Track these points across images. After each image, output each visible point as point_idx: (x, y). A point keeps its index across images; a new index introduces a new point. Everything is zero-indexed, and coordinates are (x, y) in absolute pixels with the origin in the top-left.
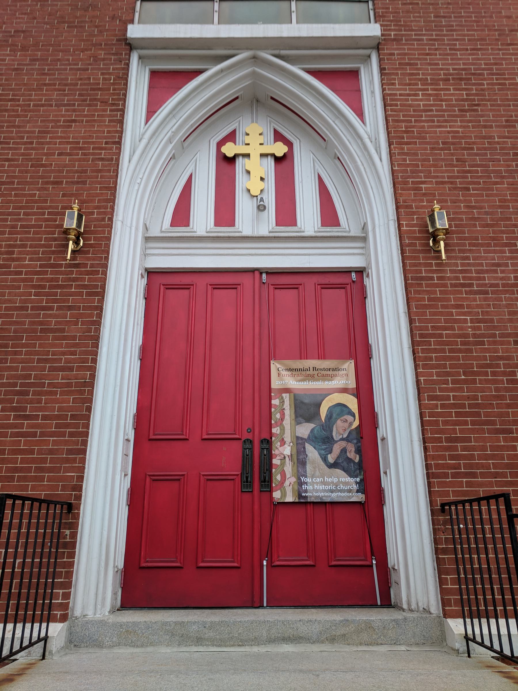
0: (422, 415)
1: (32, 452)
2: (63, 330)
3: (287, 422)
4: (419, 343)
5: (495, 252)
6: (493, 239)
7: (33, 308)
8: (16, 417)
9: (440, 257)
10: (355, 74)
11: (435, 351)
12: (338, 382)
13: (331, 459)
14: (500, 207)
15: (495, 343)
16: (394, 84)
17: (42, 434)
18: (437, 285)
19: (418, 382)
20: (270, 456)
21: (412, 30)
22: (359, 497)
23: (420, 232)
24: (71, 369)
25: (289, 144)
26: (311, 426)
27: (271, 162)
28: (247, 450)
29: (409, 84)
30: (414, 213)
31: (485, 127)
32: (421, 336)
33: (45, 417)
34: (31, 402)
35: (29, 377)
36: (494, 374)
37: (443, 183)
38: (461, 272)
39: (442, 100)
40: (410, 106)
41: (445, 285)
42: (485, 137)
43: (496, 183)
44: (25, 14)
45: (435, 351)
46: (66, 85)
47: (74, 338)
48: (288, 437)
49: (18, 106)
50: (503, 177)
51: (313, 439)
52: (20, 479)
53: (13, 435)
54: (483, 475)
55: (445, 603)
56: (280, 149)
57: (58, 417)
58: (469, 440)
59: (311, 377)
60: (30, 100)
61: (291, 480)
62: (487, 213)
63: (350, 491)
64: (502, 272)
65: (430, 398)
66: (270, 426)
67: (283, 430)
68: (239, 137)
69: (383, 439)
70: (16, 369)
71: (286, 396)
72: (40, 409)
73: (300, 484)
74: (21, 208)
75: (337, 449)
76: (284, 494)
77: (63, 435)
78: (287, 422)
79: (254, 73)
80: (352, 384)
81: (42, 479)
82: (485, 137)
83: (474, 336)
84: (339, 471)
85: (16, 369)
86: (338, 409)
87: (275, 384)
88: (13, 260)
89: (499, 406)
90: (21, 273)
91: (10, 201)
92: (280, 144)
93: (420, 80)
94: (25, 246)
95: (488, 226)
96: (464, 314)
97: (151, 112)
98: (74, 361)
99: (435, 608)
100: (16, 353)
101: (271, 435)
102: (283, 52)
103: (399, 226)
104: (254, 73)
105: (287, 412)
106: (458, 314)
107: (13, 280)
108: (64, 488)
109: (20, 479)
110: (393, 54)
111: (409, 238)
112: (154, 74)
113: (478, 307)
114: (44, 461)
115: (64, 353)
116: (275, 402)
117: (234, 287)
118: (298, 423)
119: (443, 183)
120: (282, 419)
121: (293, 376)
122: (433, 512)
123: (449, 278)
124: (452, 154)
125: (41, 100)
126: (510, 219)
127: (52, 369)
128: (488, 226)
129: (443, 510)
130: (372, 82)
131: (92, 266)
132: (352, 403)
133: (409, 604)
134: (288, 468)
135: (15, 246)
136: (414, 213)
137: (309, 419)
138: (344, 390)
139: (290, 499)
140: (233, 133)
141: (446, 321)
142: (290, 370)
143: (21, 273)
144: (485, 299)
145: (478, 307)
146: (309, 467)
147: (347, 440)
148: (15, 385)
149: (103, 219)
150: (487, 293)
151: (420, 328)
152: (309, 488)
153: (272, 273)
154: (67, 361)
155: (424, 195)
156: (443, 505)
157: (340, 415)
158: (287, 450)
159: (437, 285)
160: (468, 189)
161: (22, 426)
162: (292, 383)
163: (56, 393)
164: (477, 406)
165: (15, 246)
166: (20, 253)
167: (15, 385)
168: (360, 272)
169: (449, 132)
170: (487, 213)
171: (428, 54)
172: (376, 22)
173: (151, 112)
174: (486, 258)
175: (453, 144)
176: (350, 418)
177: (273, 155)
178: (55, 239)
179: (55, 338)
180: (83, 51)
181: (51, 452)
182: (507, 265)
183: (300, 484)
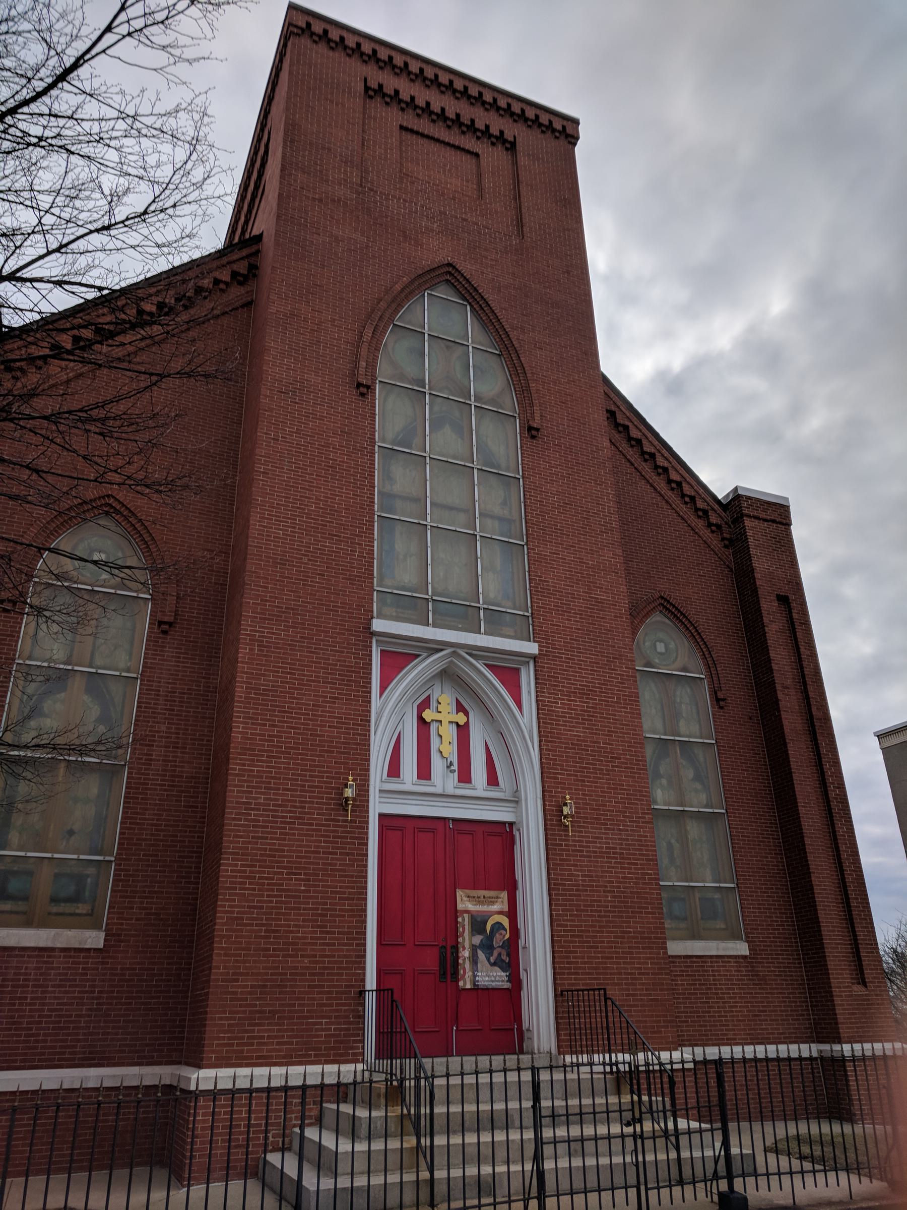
0: (552, 936)
1: (334, 956)
2: (344, 871)
3: (466, 934)
4: (554, 889)
5: (597, 828)
6: (596, 819)
7: (324, 853)
8: (321, 932)
9: (567, 831)
10: (517, 671)
11: (562, 895)
12: (496, 907)
13: (492, 960)
14: (601, 796)
15: (593, 891)
16: (544, 692)
17: (339, 944)
18: (564, 850)
19: (551, 915)
20: (458, 958)
21: (556, 649)
22: (507, 985)
23: (557, 811)
24: (353, 899)
25: (466, 714)
26: (480, 937)
27: (455, 726)
28: (597, 992)
29: (553, 694)
30: (553, 797)
31: (596, 734)
32: (555, 884)
33: (339, 933)
34: (330, 921)
35: (326, 904)
36: (591, 911)
37: (571, 775)
38: (578, 841)
39: (572, 709)
40: (553, 711)
41: (568, 850)
42: (595, 742)
43: (600, 778)
44: (292, 591)
45: (562, 895)
46: (329, 664)
47: (352, 876)
48: (467, 945)
49: (296, 679)
50: (604, 774)
51: (482, 946)
52: (328, 974)
53: (321, 944)
54: (583, 974)
55: (559, 1047)
56: (461, 719)
57: (348, 933)
58: (576, 952)
59: (481, 903)
60: (304, 675)
61: (469, 974)
62: (593, 800)
63: (503, 981)
64: (600, 843)
65: (558, 925)
66: (457, 937)
67: (464, 939)
68: (433, 704)
69: (524, 948)
70: (317, 898)
71: (466, 916)
72: (336, 927)
73: (475, 976)
74: (306, 770)
75: (495, 953)
76: (465, 983)
77: (352, 945)
78: (466, 934)
79: (452, 661)
80: (506, 908)
81: (342, 974)
82: (595, 742)
83: (583, 886)
84: (497, 968)
85: (317, 898)
86: (497, 926)
87: (460, 906)
88: (306, 813)
89: (593, 932)
90: (312, 824)
91: (298, 764)
92: (461, 714)
93: (560, 690)
94: (313, 802)
95: (594, 809)
96: (578, 871)
97: (383, 689)
98: (354, 893)
99: (554, 1051)
100: (315, 886)
101: (457, 943)
102: (474, 652)
103: (544, 805)
104: (452, 661)
105: (467, 927)
106: (575, 870)
107: (308, 830)
108: (356, 980)
109: (328, 974)
110: (544, 667)
111: (551, 815)
112: (382, 651)
113: (586, 866)
114: (342, 962)
115: (347, 887)
116: (460, 920)
117: (433, 831)
118: (473, 935)
119: (571, 775)
120: (464, 931)
121: (470, 901)
122: (556, 996)
123: (571, 846)
124: (577, 753)
125: (311, 676)
126: (605, 806)
127: (340, 899)
128: (594, 809)
129: (562, 995)
130: (529, 683)
131: (360, 822)
132: (505, 921)
133: (539, 1049)
134: (467, 966)
135: (306, 802)
136: (553, 797)
137: (479, 933)
138: (500, 913)
139: (468, 986)
140: (428, 699)
141: (568, 875)
142: (469, 897)
143: (312, 824)
144: (590, 861)
145: (586, 866)
146: (479, 965)
147: (502, 947)
148: (317, 909)
149: (364, 785)
150: (590, 857)
151: (554, 879)
152: (480, 979)
153: (455, 820)
154: (350, 893)
155: (560, 783)
156: (562, 991)
157: (498, 930)
158: (466, 954)
159: (564, 850)
160: (584, 781)
161: (325, 938)
162: (471, 907)
163: (344, 916)
164: (582, 931)
165: (306, 802)
166: (310, 808)
167: (317, 909)
168: (511, 824)
169: (575, 736)
170: (593, 800)
171: (565, 670)
172: (534, 641)
173: (383, 689)
174: (591, 833)
175: (577, 745)
176: (503, 932)
177: (457, 724)
178: (332, 799)
179: (341, 876)
180: (339, 634)
181: (345, 956)
182: (602, 838)
183: (475, 976)
